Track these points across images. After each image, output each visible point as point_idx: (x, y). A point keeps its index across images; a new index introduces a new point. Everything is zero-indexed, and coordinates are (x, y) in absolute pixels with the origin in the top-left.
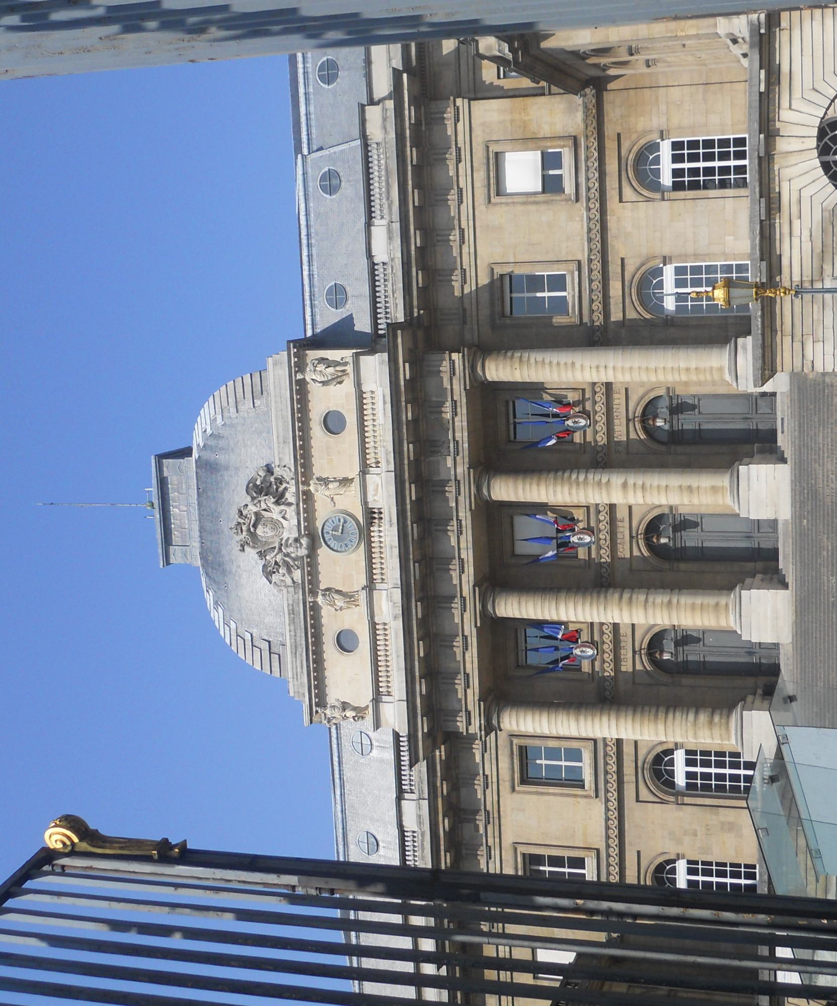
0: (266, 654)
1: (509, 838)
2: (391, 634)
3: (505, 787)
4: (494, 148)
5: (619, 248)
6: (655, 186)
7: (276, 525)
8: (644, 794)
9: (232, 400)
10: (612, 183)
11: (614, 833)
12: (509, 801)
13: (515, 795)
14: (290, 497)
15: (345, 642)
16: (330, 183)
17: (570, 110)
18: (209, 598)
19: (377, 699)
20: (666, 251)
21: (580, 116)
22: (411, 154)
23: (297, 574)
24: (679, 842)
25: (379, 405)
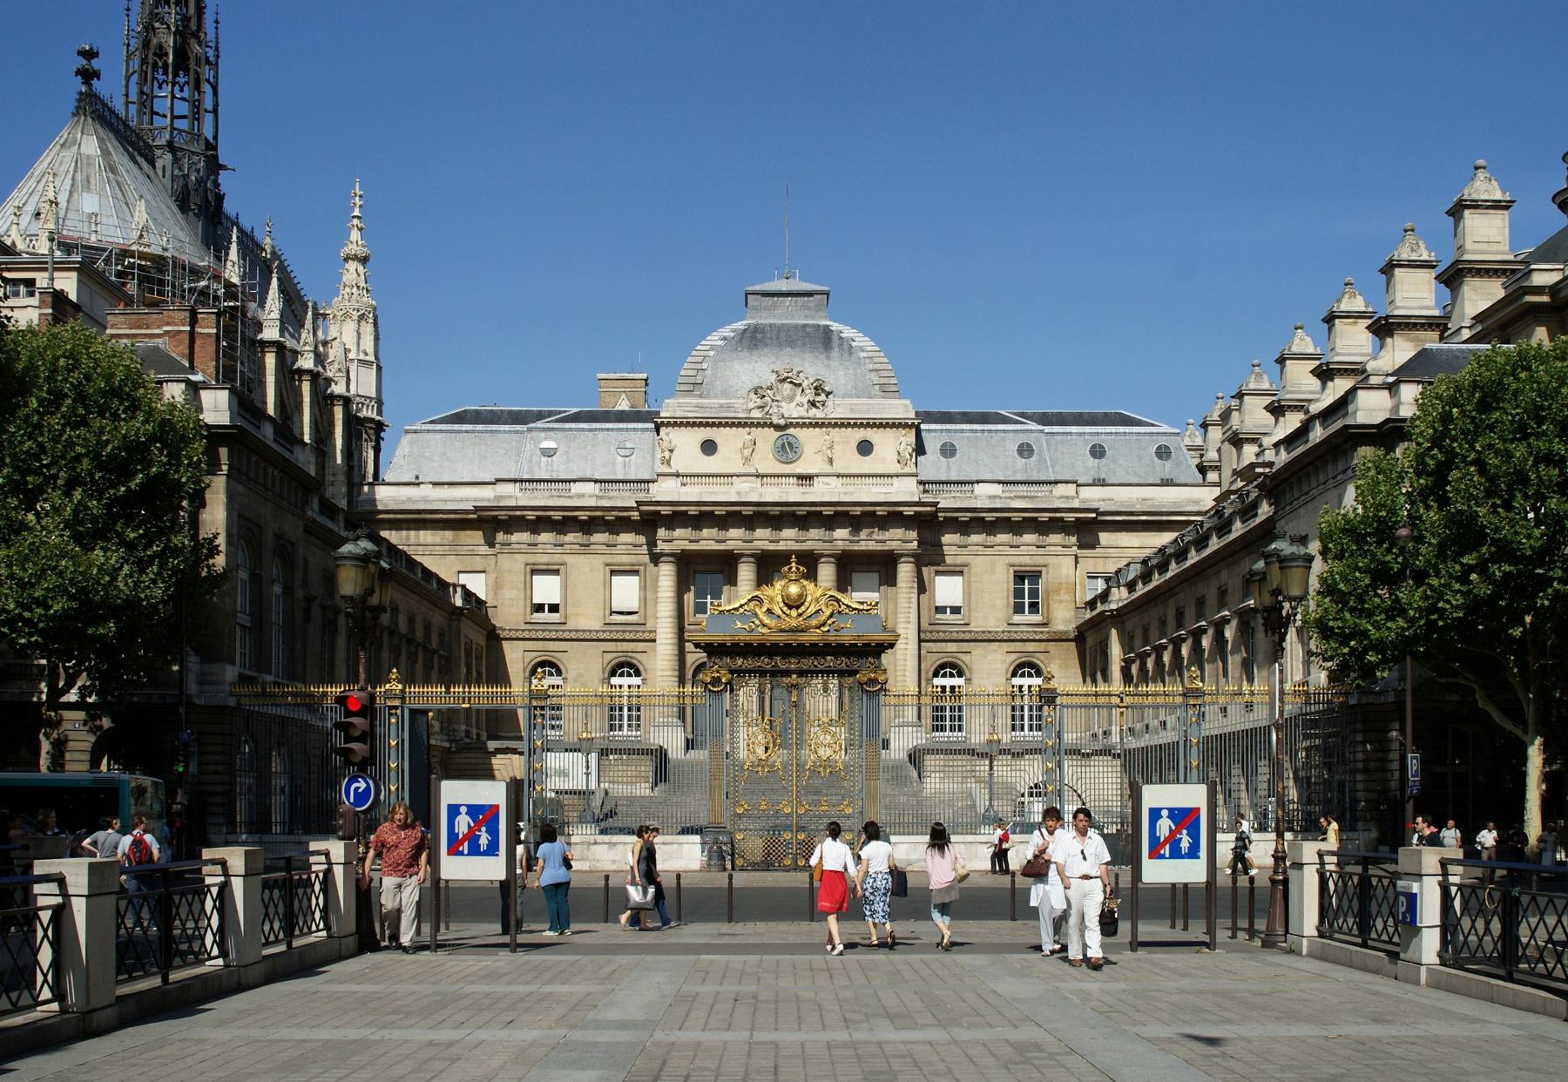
0: (692, 380)
1: (569, 559)
2: (725, 488)
3: (609, 559)
4: (1044, 570)
5: (978, 650)
6: (1014, 674)
7: (791, 398)
8: (610, 656)
9: (878, 366)
10: (1018, 646)
11: (581, 635)
12: (597, 562)
13: (601, 567)
14: (813, 412)
15: (709, 447)
16: (1025, 450)
17: (1066, 622)
18: (727, 331)
19: (678, 475)
20: (975, 681)
21: (1061, 627)
22: (1045, 517)
23: (757, 414)
24: (576, 680)
25: (884, 490)
